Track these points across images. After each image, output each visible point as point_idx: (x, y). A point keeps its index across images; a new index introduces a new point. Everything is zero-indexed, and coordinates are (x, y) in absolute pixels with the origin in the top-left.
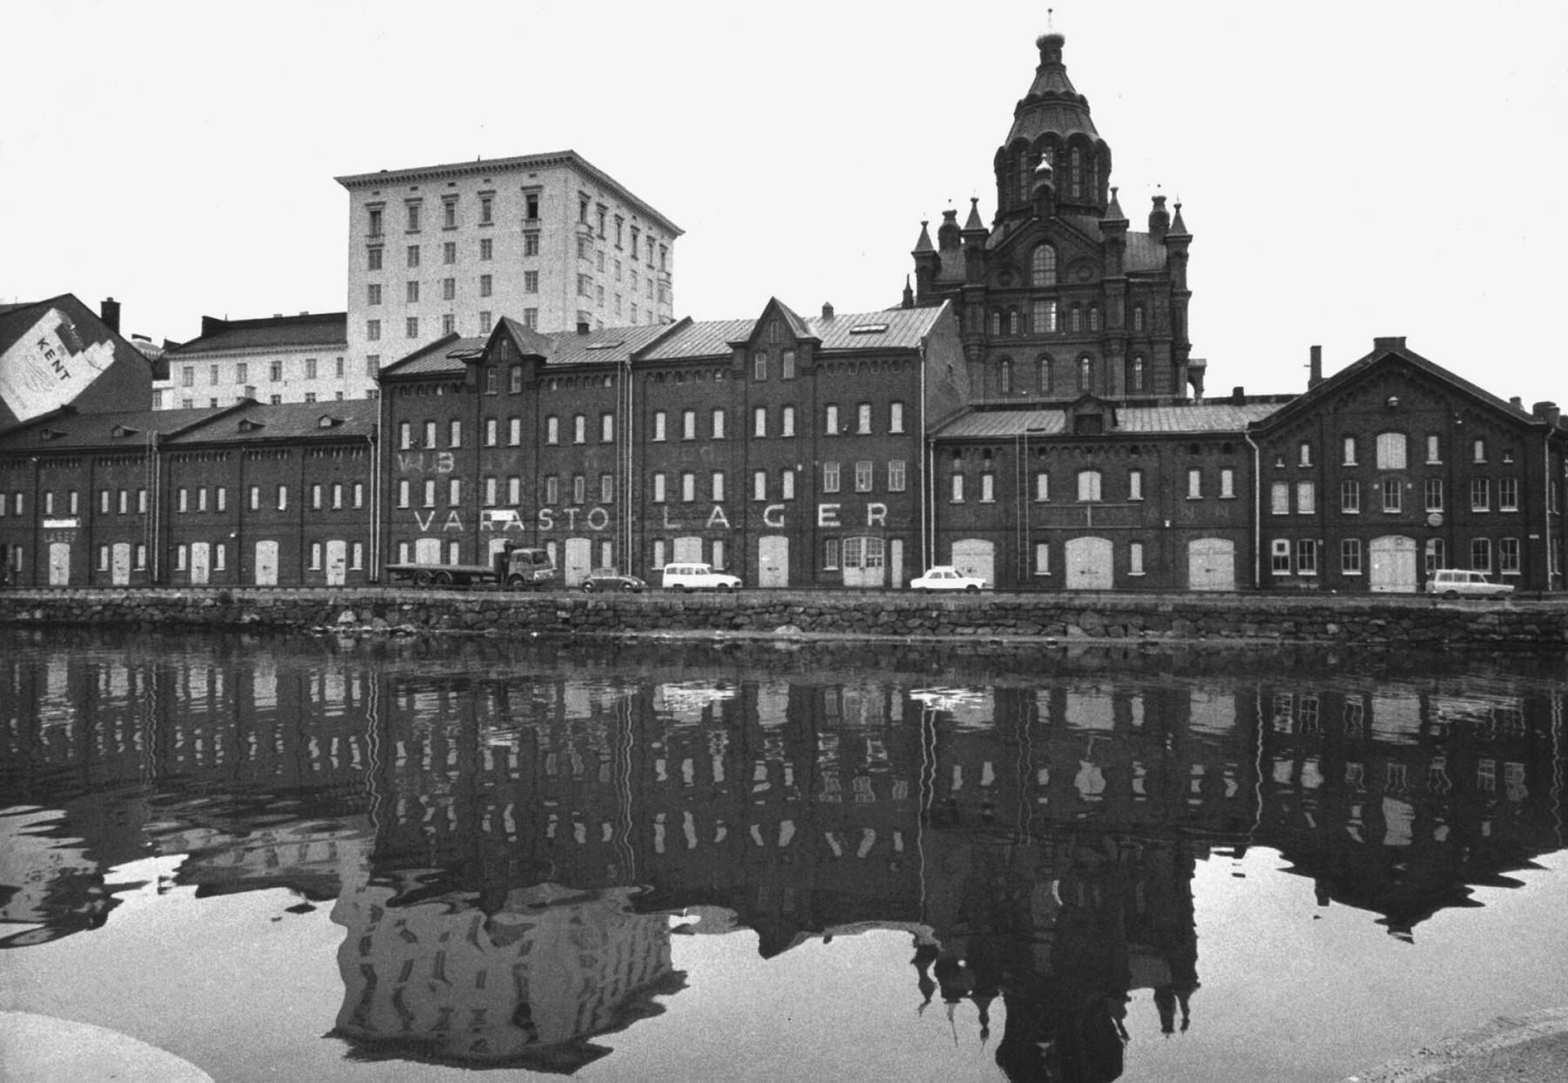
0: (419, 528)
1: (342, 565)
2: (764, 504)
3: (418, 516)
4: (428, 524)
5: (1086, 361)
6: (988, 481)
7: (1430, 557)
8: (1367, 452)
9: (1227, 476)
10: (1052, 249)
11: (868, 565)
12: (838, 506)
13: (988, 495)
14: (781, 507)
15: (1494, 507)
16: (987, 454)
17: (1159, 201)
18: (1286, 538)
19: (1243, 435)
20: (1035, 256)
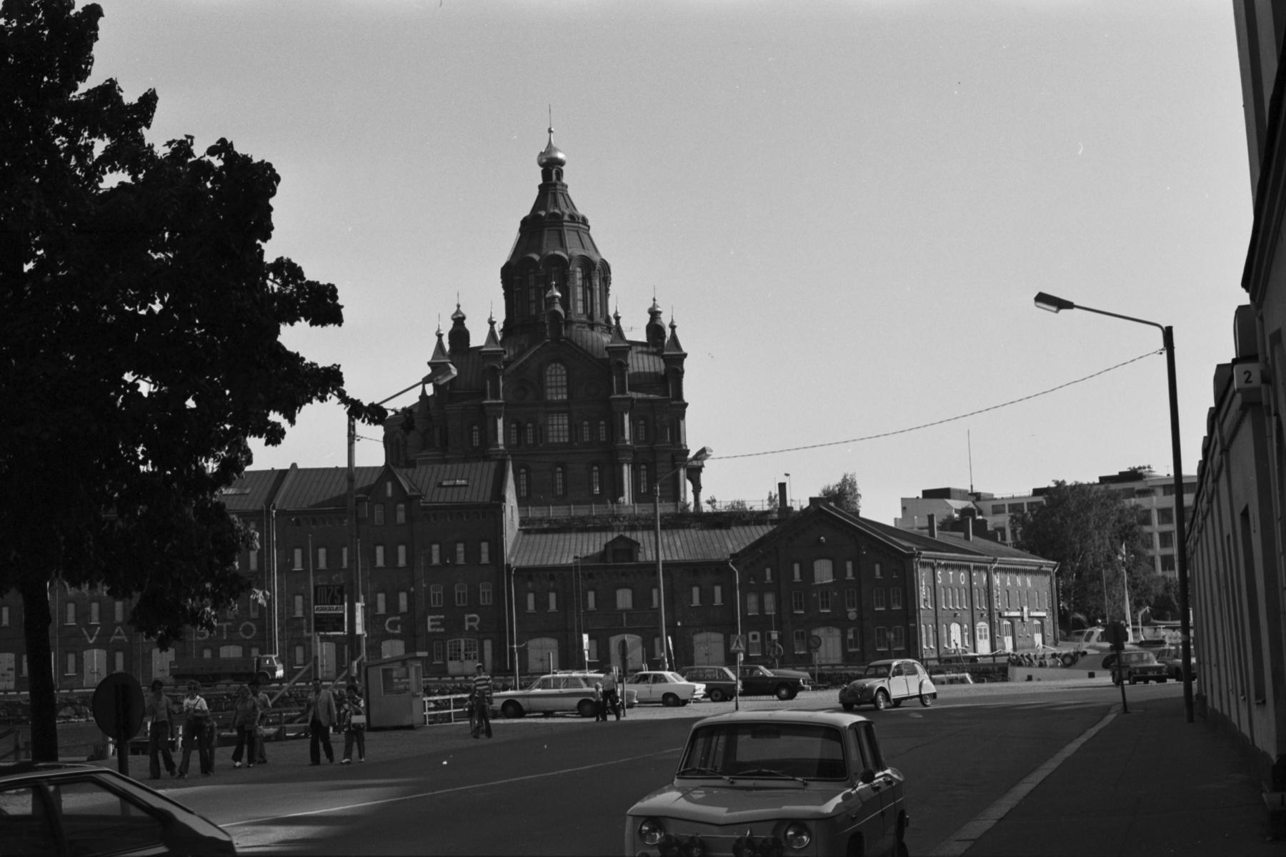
0: (87, 641)
1: (12, 674)
2: (385, 617)
3: (85, 632)
4: (94, 638)
5: (596, 468)
6: (552, 597)
7: (850, 640)
8: (808, 573)
9: (718, 590)
10: (562, 368)
11: (466, 659)
12: (443, 617)
13: (553, 607)
14: (398, 618)
15: (888, 607)
16: (552, 578)
17: (654, 314)
18: (758, 630)
19: (726, 562)
20: (548, 373)
